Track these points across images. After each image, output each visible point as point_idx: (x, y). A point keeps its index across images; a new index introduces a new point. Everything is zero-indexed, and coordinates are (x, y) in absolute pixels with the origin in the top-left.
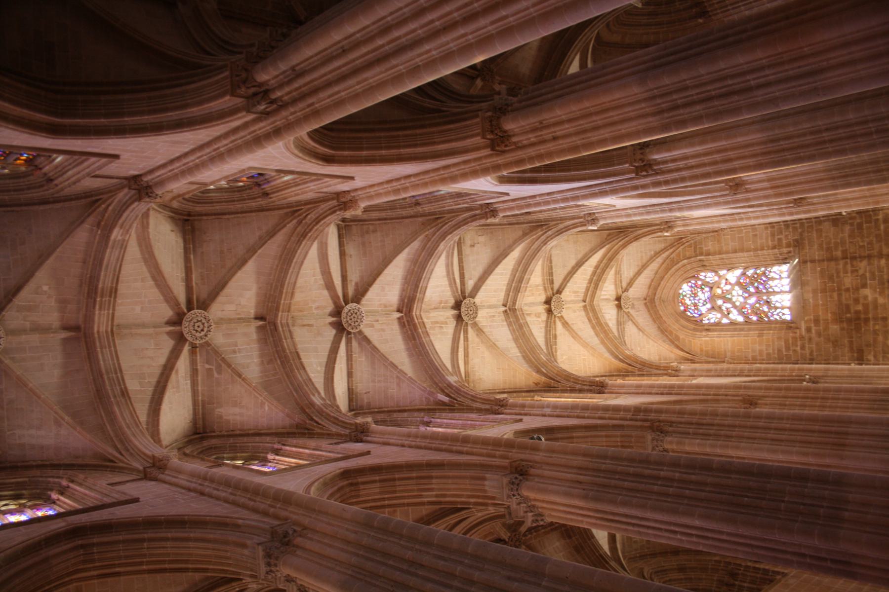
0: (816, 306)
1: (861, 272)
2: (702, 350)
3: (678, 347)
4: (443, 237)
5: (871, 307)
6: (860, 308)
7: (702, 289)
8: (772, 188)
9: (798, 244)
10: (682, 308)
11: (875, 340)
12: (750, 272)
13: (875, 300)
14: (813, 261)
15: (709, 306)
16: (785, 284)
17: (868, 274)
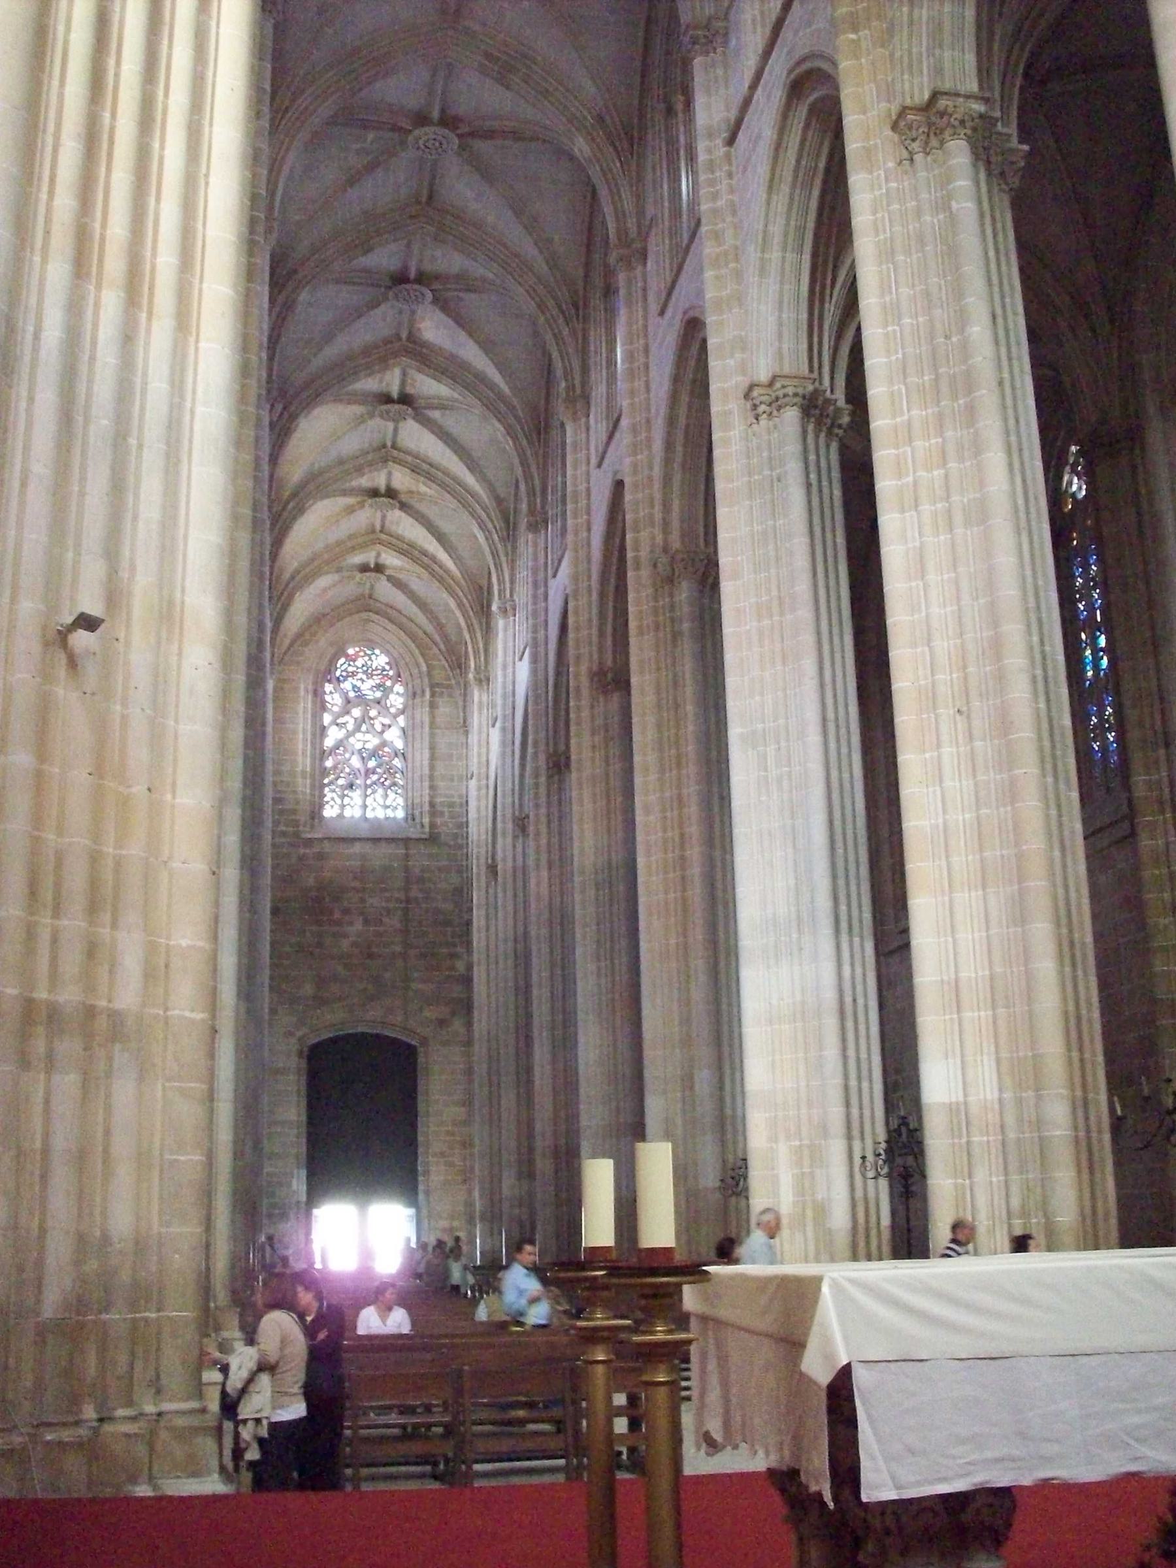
1: (386, 920)
2: (284, 681)
5: (336, 929)
6: (337, 915)
7: (378, 686)
9: (433, 839)
10: (351, 651)
12: (397, 762)
13: (345, 936)
14: (407, 855)
15: (352, 694)
16: (377, 812)
17: (382, 929)
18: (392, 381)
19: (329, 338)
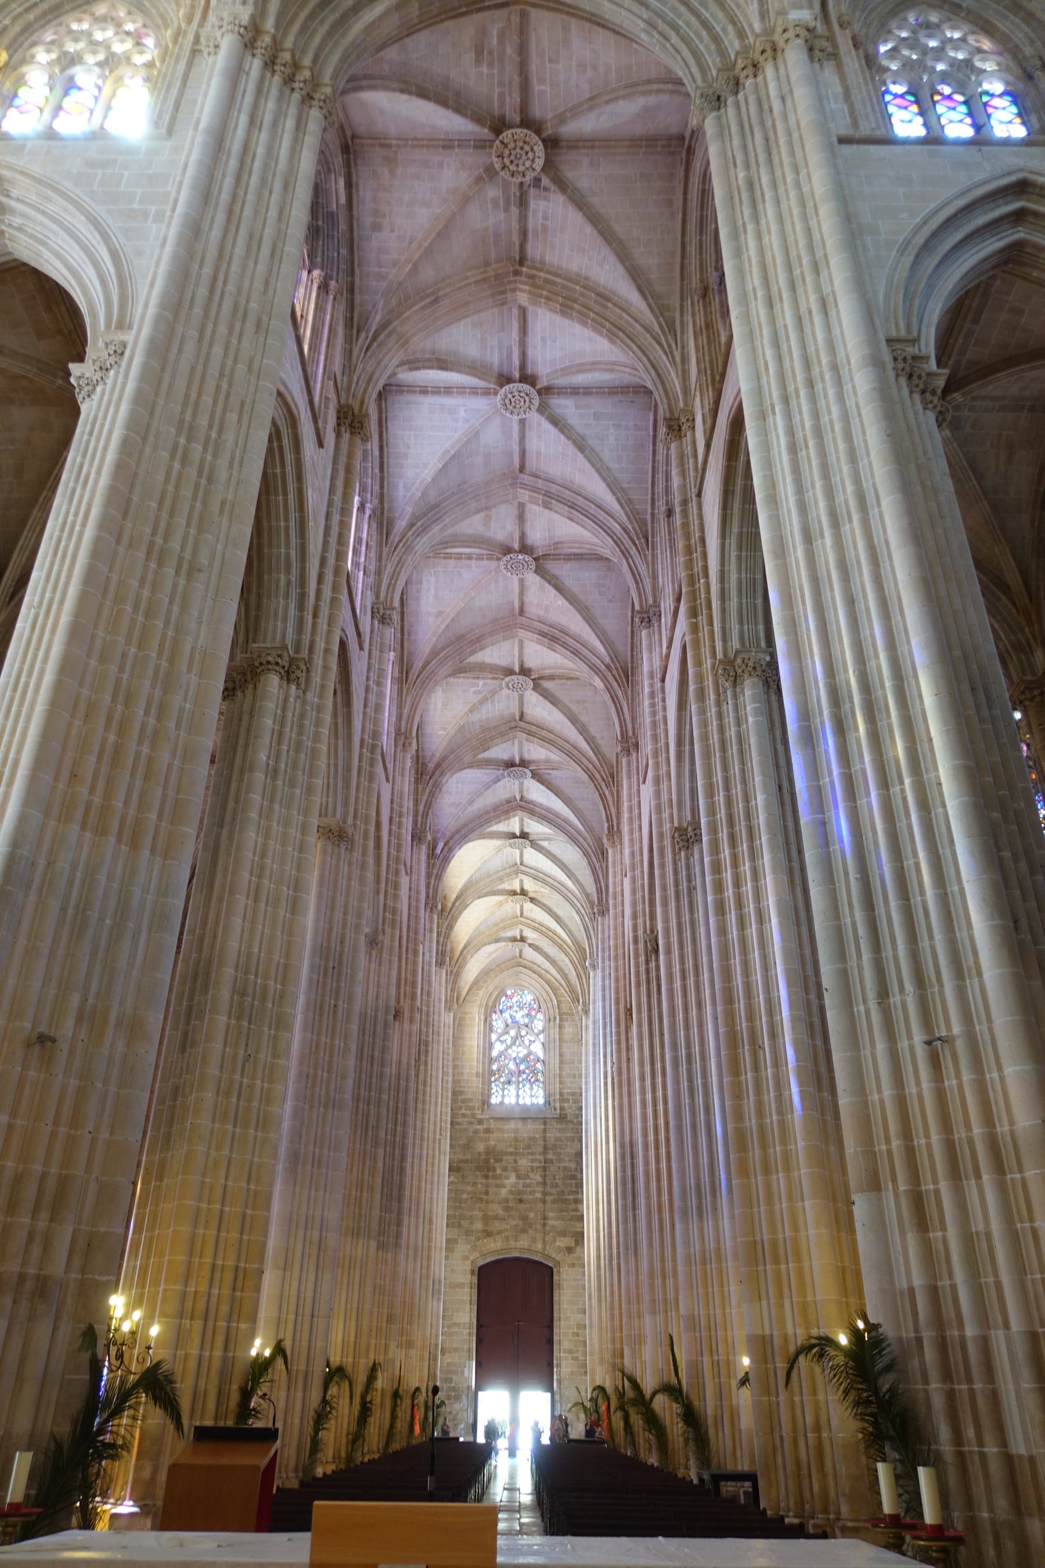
0: (502, 1131)
3: (470, 989)
4: (586, 854)
5: (498, 1182)
6: (498, 1172)
9: (562, 1118)
10: (509, 993)
11: (468, 1183)
12: (539, 1066)
14: (545, 1131)
18: (514, 825)
19: (471, 802)
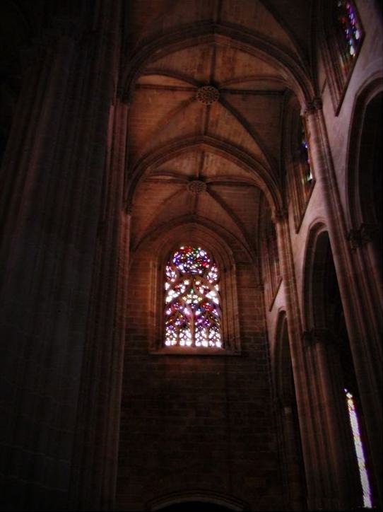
8: (356, 276)
9: (244, 356)
10: (182, 248)
